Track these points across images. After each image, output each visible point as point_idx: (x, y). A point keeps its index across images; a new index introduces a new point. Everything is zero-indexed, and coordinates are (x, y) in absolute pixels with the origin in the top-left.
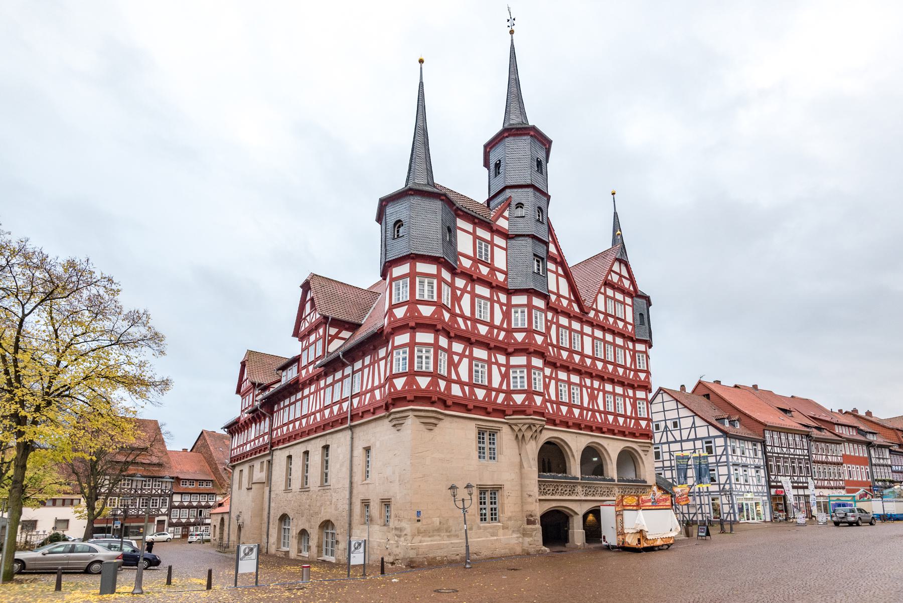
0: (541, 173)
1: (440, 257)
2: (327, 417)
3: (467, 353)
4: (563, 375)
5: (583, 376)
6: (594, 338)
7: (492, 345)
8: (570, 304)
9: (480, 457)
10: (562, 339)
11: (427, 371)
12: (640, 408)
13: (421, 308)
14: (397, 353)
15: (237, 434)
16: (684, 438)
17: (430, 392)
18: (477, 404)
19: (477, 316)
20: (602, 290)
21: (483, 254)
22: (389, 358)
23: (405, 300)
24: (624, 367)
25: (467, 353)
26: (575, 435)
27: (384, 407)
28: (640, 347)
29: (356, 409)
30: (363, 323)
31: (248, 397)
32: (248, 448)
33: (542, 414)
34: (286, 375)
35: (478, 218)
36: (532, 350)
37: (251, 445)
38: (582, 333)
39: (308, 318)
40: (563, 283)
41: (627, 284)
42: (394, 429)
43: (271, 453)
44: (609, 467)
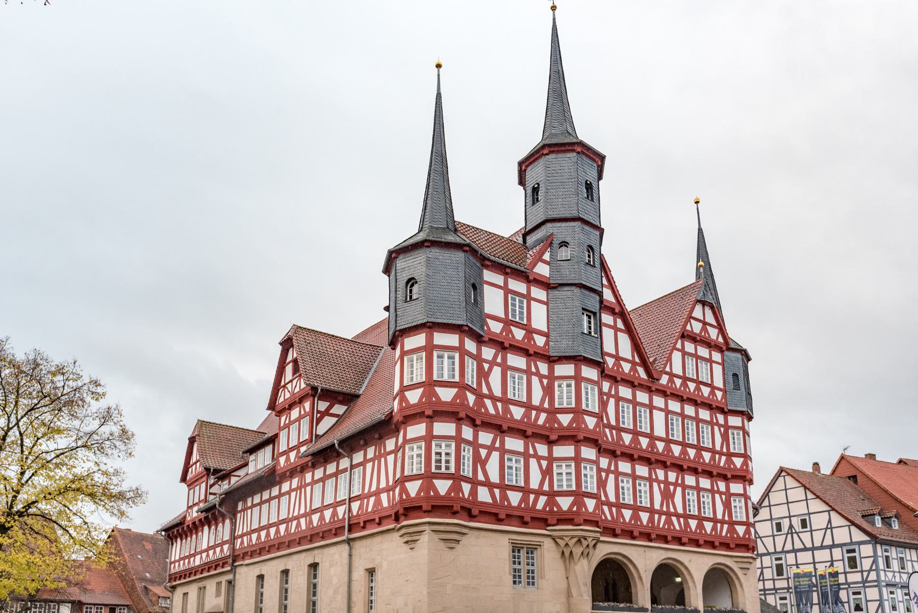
0: (592, 200)
1: (463, 325)
2: (315, 525)
3: (497, 445)
4: (624, 467)
5: (652, 466)
6: (667, 412)
7: (529, 433)
8: (633, 369)
9: (515, 582)
10: (623, 417)
11: (447, 472)
12: (735, 507)
13: (439, 390)
14: (409, 448)
15: (179, 540)
16: (817, 544)
17: (452, 499)
18: (509, 512)
19: (510, 396)
20: (679, 346)
21: (517, 313)
22: (400, 454)
23: (419, 380)
24: (713, 451)
25: (497, 445)
26: (642, 549)
27: (393, 517)
28: (735, 421)
29: (355, 516)
30: (361, 392)
31: (198, 487)
32: (197, 561)
33: (596, 523)
34: (255, 460)
35: (509, 267)
36: (581, 437)
37: (201, 558)
38: (651, 407)
39: (289, 386)
40: (625, 342)
41: (713, 333)
42: (406, 548)
43: (233, 570)
44: (692, 592)
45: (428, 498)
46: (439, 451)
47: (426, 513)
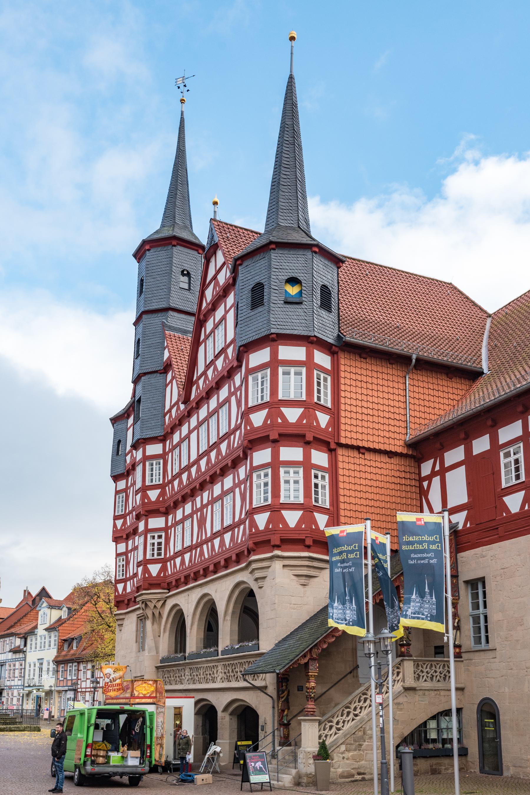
13: (285, 411)
46: (287, 479)
47: (275, 548)
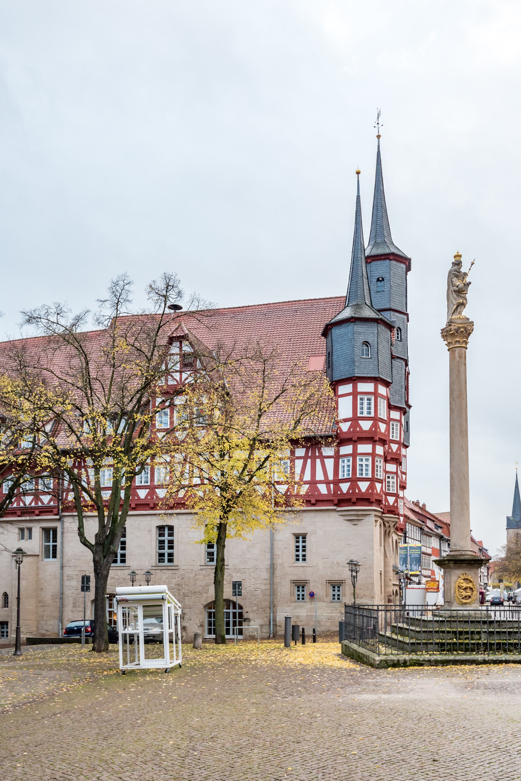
45: (372, 494)
